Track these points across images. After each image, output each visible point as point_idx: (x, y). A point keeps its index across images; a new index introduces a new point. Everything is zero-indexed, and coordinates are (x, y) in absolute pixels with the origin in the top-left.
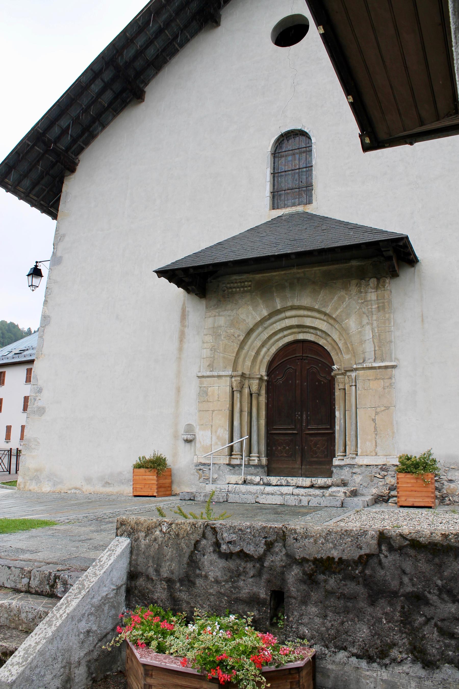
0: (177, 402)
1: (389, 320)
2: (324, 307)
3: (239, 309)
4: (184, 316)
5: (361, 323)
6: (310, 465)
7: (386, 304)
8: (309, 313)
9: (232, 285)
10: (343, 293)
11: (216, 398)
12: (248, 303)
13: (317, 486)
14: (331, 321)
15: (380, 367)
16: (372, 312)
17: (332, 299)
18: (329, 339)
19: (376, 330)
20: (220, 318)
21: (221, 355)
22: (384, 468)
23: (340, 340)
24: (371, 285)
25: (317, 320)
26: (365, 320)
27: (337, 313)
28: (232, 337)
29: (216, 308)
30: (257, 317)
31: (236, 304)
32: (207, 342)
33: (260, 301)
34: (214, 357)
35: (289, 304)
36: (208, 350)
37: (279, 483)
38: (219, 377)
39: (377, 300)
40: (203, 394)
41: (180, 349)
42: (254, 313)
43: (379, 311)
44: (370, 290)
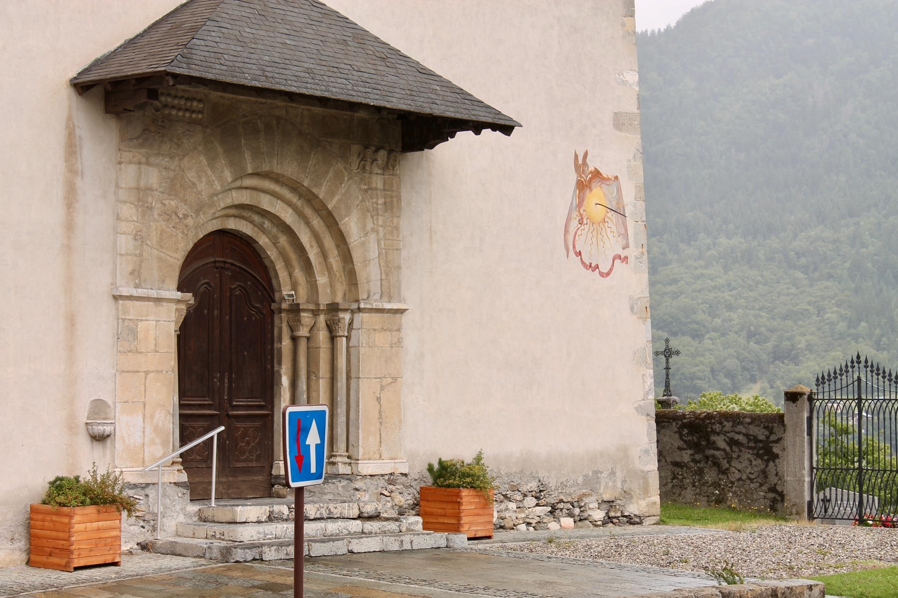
0: (71, 348)
1: (397, 228)
2: (315, 186)
3: (184, 156)
4: (72, 149)
5: (364, 226)
6: (233, 476)
7: (395, 199)
8: (277, 188)
9: (169, 100)
10: (340, 166)
11: (152, 347)
12: (200, 148)
13: (366, 515)
14: (308, 211)
15: (390, 311)
16: (377, 209)
17: (327, 172)
18: (283, 240)
19: (382, 243)
20: (150, 169)
21: (155, 252)
22: (391, 479)
23: (312, 246)
24: (380, 162)
25: (279, 202)
26: (370, 225)
27: (334, 202)
28: (174, 217)
29: (142, 146)
30: (216, 183)
31: (179, 146)
32: (127, 220)
33: (220, 150)
34: (141, 255)
35: (266, 167)
36: (130, 238)
37: (318, 516)
38: (158, 300)
39: (384, 190)
40: (126, 335)
41: (70, 227)
42: (210, 173)
43: (386, 211)
44: (376, 170)
